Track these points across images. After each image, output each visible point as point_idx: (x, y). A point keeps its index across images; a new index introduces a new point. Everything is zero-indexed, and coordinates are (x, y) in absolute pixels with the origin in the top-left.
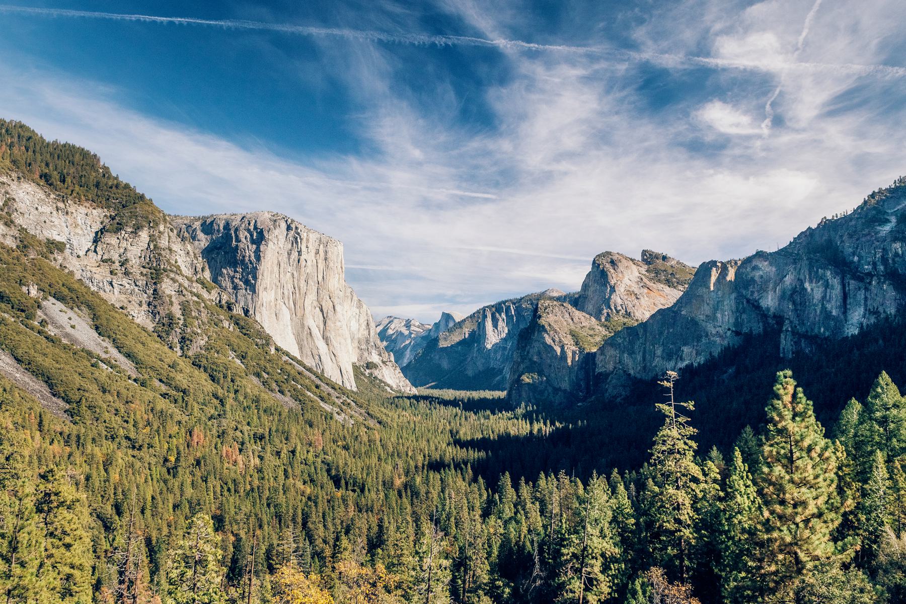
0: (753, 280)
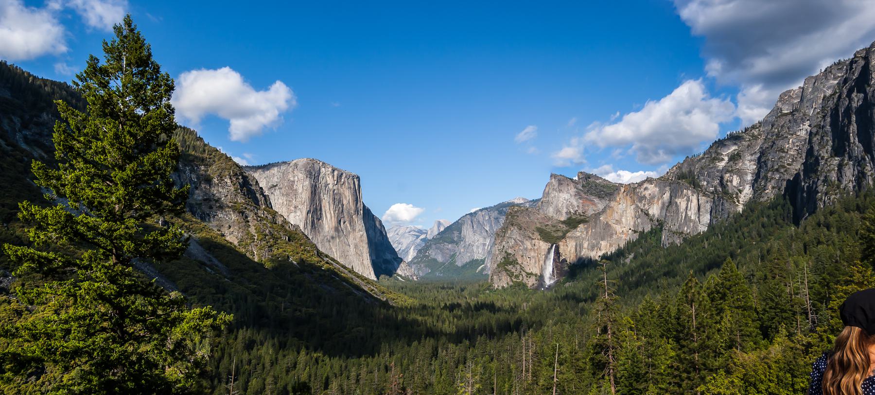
0: (644, 197)
